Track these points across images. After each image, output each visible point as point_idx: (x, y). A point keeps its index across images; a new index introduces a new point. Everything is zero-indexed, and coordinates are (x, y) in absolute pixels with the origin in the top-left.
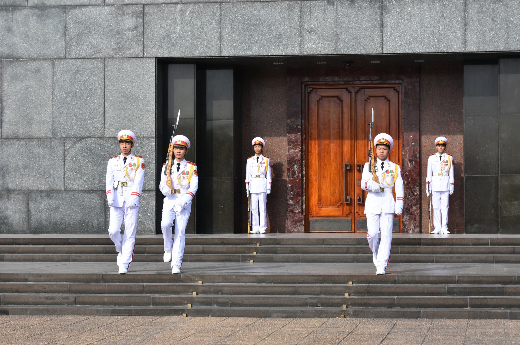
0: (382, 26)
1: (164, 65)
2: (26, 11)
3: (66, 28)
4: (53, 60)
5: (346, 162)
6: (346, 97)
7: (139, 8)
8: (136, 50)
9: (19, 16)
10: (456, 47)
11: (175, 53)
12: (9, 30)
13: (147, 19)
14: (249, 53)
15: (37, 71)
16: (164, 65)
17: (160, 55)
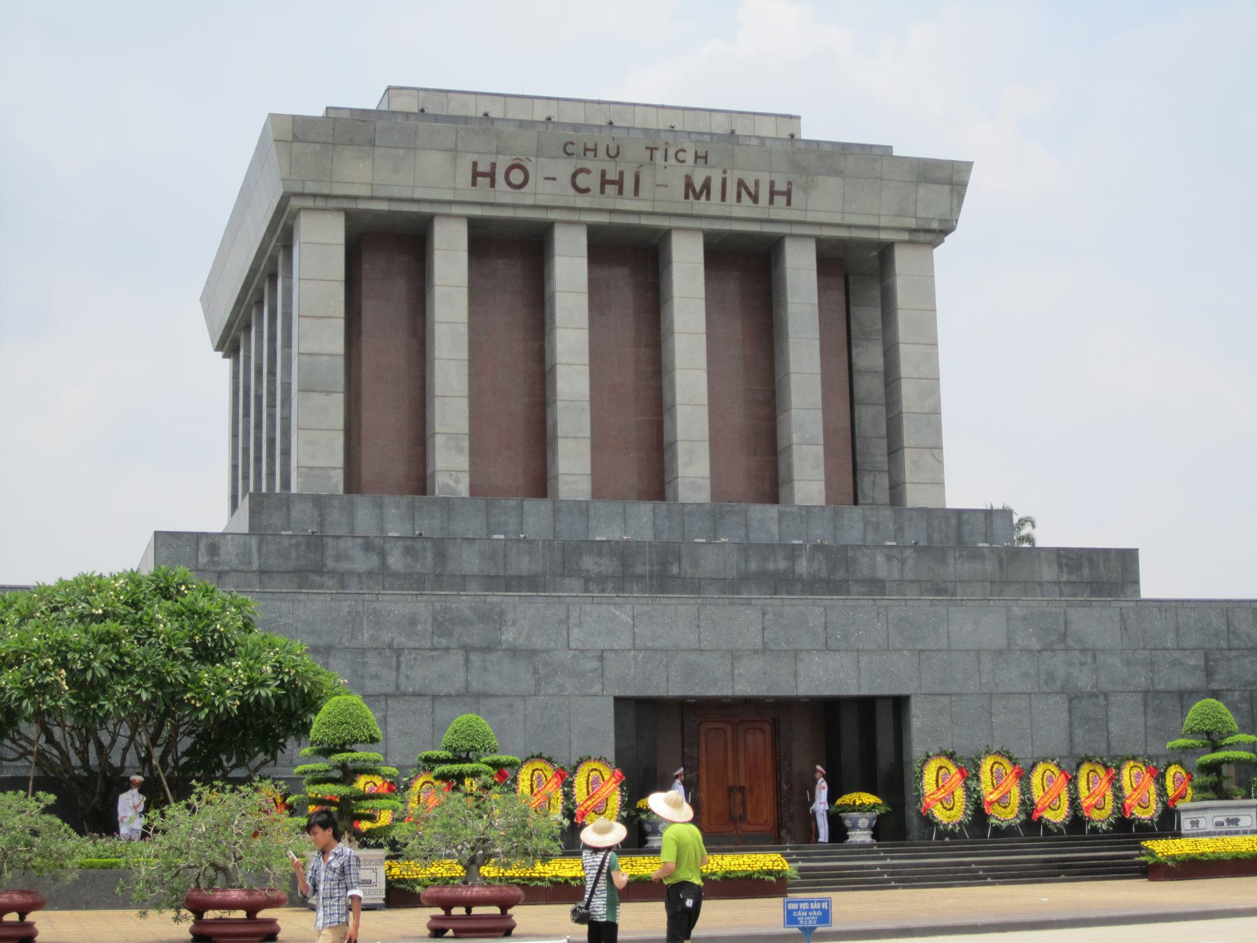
0: (795, 674)
2: (500, 653)
3: (536, 671)
4: (523, 697)
5: (731, 783)
6: (729, 729)
7: (598, 654)
8: (597, 689)
9: (494, 657)
10: (853, 692)
11: (630, 693)
12: (485, 669)
13: (606, 662)
14: (691, 693)
15: (511, 706)
17: (617, 694)
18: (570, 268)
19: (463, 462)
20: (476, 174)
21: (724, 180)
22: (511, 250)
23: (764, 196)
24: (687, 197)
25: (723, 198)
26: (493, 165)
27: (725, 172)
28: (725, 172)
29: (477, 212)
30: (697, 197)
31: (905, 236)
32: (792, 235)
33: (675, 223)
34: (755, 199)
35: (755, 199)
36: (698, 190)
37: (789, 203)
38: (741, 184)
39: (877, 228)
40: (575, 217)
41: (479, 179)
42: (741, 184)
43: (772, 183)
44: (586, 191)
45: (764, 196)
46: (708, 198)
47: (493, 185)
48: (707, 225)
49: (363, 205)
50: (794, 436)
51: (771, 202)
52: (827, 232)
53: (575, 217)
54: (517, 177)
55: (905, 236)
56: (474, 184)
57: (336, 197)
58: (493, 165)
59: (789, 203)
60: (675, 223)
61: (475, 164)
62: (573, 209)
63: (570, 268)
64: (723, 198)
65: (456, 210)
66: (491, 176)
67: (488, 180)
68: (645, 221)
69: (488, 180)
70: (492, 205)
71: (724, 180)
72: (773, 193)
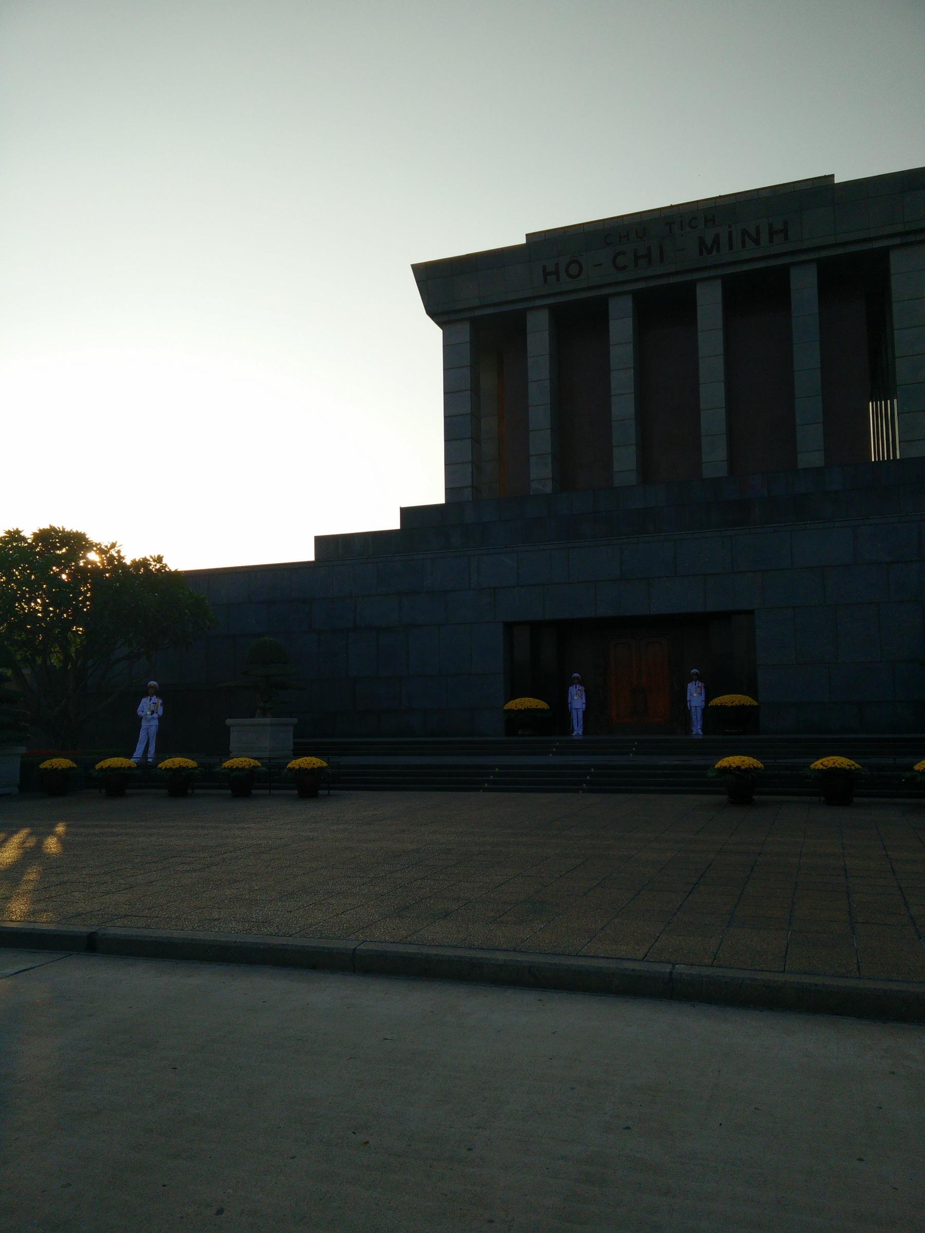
1: (509, 627)
16: (509, 627)
18: (621, 327)
19: (547, 472)
20: (546, 274)
21: (730, 233)
22: (580, 322)
23: (764, 237)
24: (701, 253)
25: (731, 247)
26: (557, 265)
27: (730, 226)
28: (730, 226)
29: (551, 301)
30: (710, 252)
31: (897, 241)
32: (794, 264)
33: (696, 276)
34: (757, 242)
35: (757, 242)
36: (709, 246)
37: (786, 238)
38: (745, 233)
39: (869, 240)
40: (620, 289)
41: (548, 277)
42: (745, 233)
43: (771, 225)
44: (625, 267)
45: (764, 237)
46: (718, 251)
47: (558, 280)
48: (719, 272)
49: (478, 313)
50: (798, 420)
51: (771, 241)
52: (824, 254)
53: (620, 289)
54: (574, 269)
55: (897, 241)
56: (545, 281)
57: (461, 311)
58: (557, 265)
59: (786, 238)
60: (696, 276)
61: (544, 268)
62: (617, 284)
63: (621, 327)
64: (731, 247)
65: (539, 303)
66: (556, 273)
67: (554, 277)
68: (672, 280)
69: (554, 277)
70: (561, 293)
71: (730, 233)
72: (772, 234)
